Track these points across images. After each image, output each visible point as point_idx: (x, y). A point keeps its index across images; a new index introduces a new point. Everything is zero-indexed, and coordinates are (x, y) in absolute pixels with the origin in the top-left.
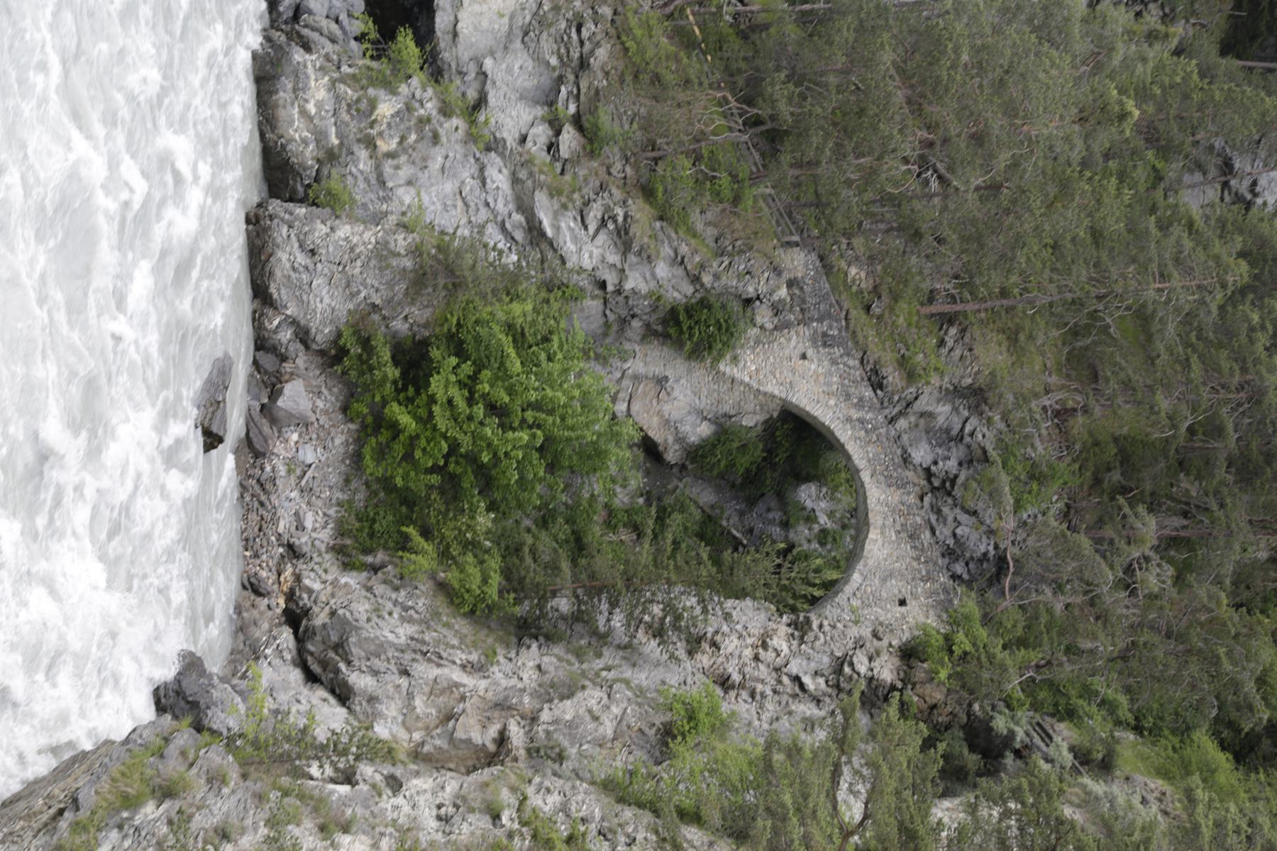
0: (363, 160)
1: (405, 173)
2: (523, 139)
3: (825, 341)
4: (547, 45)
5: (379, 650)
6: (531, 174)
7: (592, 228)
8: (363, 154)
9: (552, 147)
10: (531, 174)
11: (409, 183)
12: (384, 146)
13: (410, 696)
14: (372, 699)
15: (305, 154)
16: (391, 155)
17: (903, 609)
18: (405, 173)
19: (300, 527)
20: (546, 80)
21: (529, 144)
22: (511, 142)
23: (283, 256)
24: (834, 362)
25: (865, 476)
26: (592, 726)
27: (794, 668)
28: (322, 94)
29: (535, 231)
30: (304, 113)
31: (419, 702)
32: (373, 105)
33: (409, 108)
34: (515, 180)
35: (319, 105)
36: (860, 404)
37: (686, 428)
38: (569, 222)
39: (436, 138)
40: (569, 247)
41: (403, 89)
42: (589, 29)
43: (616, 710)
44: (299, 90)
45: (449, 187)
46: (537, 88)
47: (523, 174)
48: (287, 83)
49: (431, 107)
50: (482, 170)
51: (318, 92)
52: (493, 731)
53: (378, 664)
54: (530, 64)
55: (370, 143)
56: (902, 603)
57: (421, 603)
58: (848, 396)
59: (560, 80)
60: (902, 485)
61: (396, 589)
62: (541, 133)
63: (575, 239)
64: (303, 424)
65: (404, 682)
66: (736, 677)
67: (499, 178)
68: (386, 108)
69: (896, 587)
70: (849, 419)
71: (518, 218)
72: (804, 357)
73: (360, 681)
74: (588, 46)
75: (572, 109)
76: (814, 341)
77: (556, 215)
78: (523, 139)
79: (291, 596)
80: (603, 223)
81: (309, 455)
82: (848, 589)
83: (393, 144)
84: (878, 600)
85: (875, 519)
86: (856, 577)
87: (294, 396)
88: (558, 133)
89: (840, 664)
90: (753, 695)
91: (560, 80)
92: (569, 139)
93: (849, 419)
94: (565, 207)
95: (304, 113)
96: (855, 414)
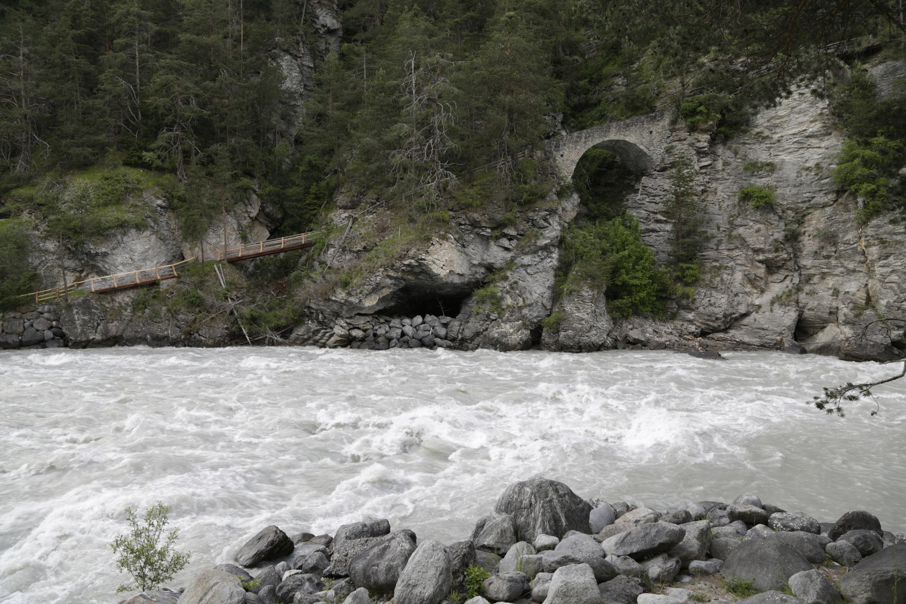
0: (525, 311)
1: (528, 295)
2: (507, 249)
3: (557, 146)
4: (467, 238)
5: (730, 303)
6: (529, 246)
7: (546, 224)
8: (525, 311)
9: (511, 239)
10: (529, 246)
11: (531, 294)
12: (521, 303)
13: (746, 293)
14: (748, 306)
15: (524, 334)
16: (524, 301)
17: (654, 133)
18: (528, 295)
19: (671, 333)
20: (478, 240)
21: (510, 247)
22: (509, 255)
23: (593, 339)
24: (565, 145)
25: (606, 139)
26: (763, 232)
27: (697, 168)
28: (508, 326)
29: (545, 248)
30: (511, 334)
31: (747, 290)
32: (508, 306)
33: (508, 292)
34: (527, 254)
35: (511, 327)
36: (580, 138)
37: (576, 203)
38: (547, 233)
39: (516, 283)
40: (554, 234)
41: (499, 294)
42: (460, 220)
43: (751, 224)
44: (505, 335)
45: (529, 278)
46: (481, 244)
47: (527, 250)
48: (504, 340)
49: (506, 284)
50: (523, 266)
51: (507, 328)
52: (760, 265)
53: (735, 303)
54: (472, 246)
55: (520, 308)
56: (651, 132)
57: (703, 291)
58: (577, 142)
59: (478, 234)
60: (609, 127)
61: (695, 299)
62: (505, 242)
63: (552, 231)
64: (643, 332)
65: (741, 295)
66: (702, 188)
67: (527, 259)
68: (509, 301)
69: (646, 134)
70: (585, 142)
71: (540, 253)
72: (562, 156)
73: (742, 309)
74: (467, 222)
75: (489, 230)
76: (557, 151)
77: (544, 238)
78: (507, 249)
79: (696, 336)
80: (546, 220)
81: (650, 330)
82: (646, 150)
83: (521, 299)
84: (651, 141)
85: (621, 138)
86: (642, 147)
87: (635, 334)
88: (505, 235)
89: (700, 153)
90: (708, 182)
91: (478, 234)
92: (511, 232)
93: (585, 142)
94: (542, 234)
95: (511, 334)
96: (583, 140)
